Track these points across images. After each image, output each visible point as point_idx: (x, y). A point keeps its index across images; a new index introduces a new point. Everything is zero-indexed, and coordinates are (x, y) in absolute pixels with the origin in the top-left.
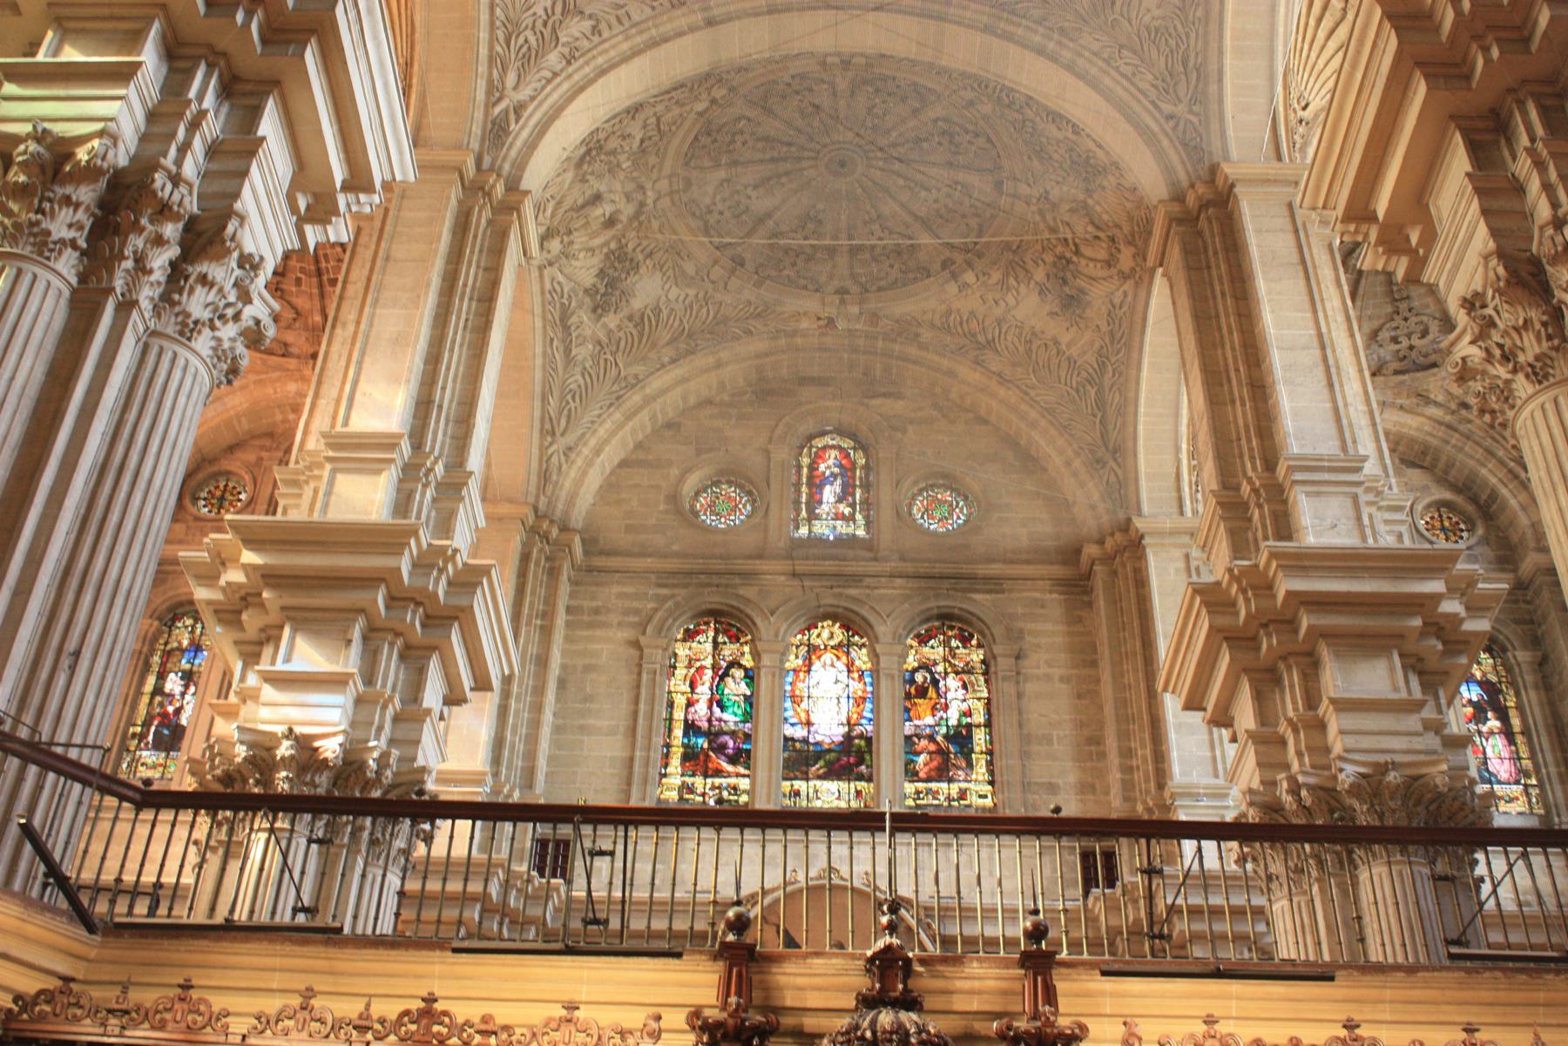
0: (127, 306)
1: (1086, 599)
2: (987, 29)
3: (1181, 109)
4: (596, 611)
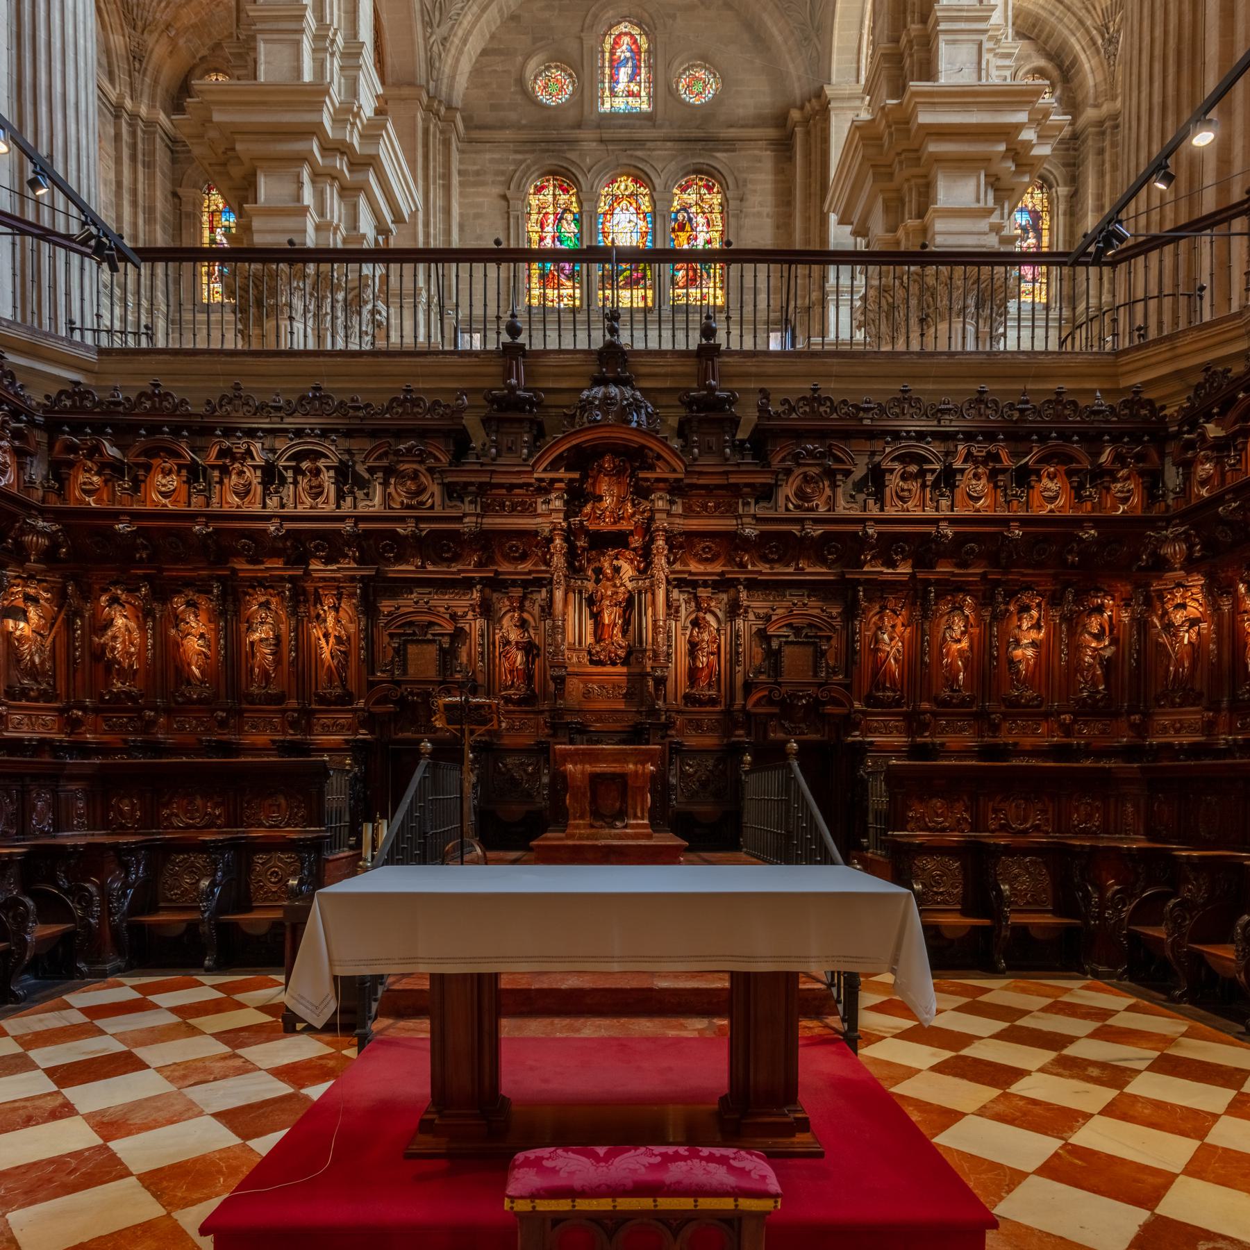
4: (477, 173)
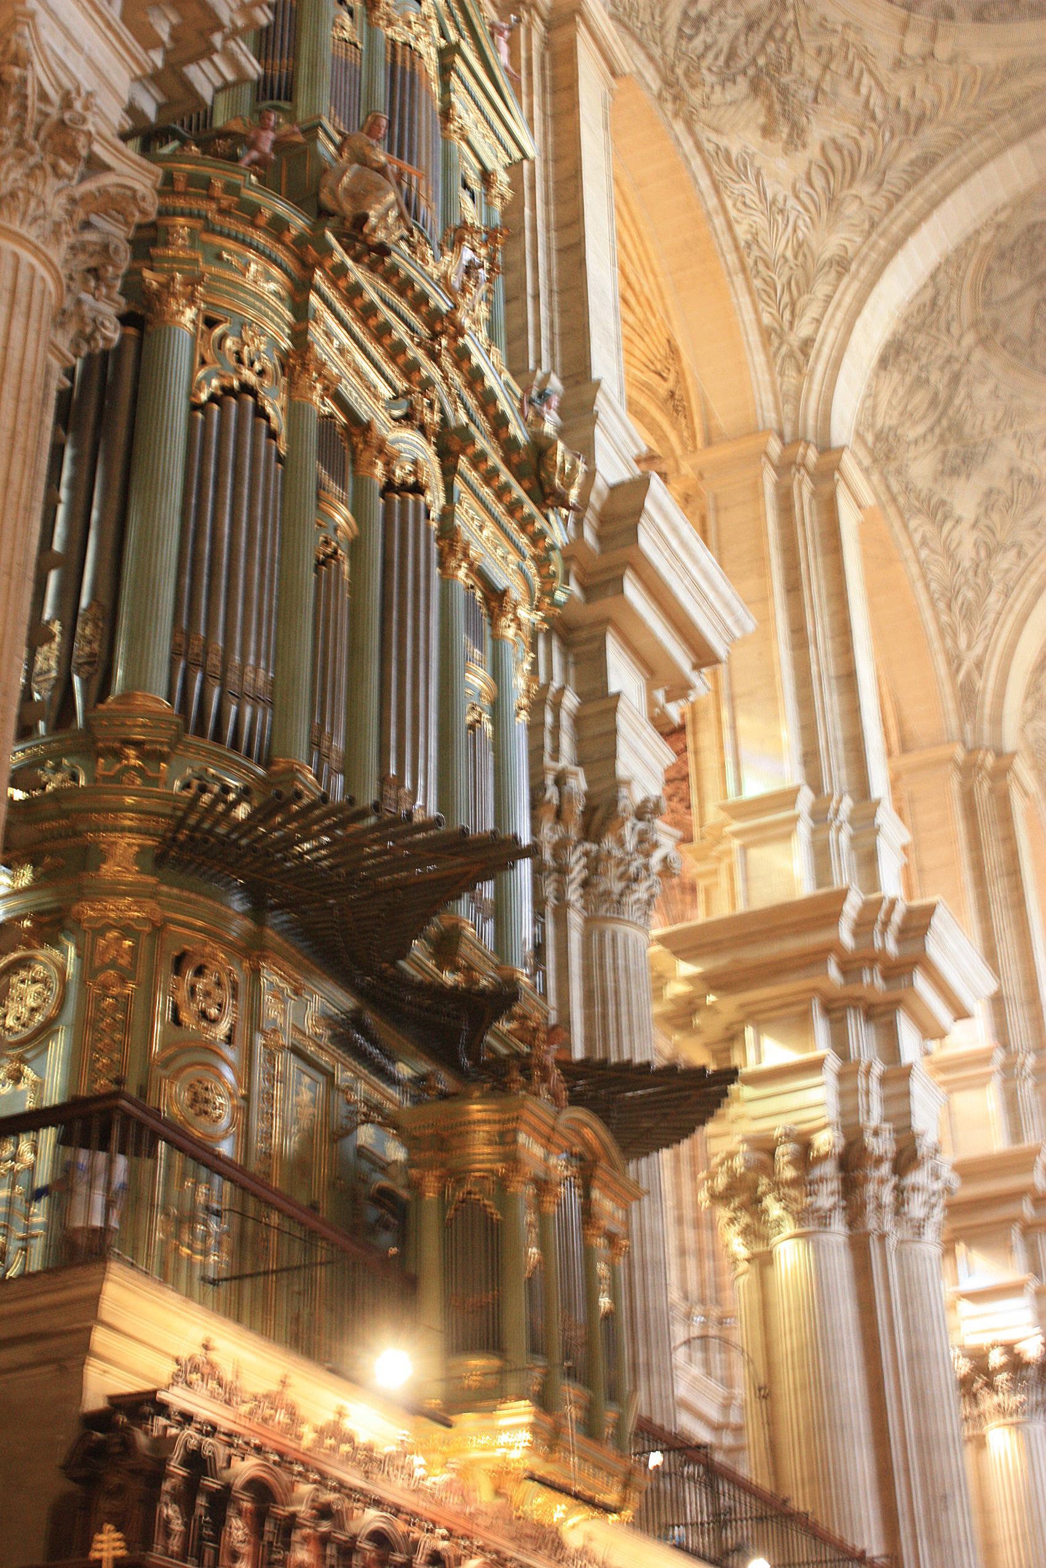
0: (882, 1237)
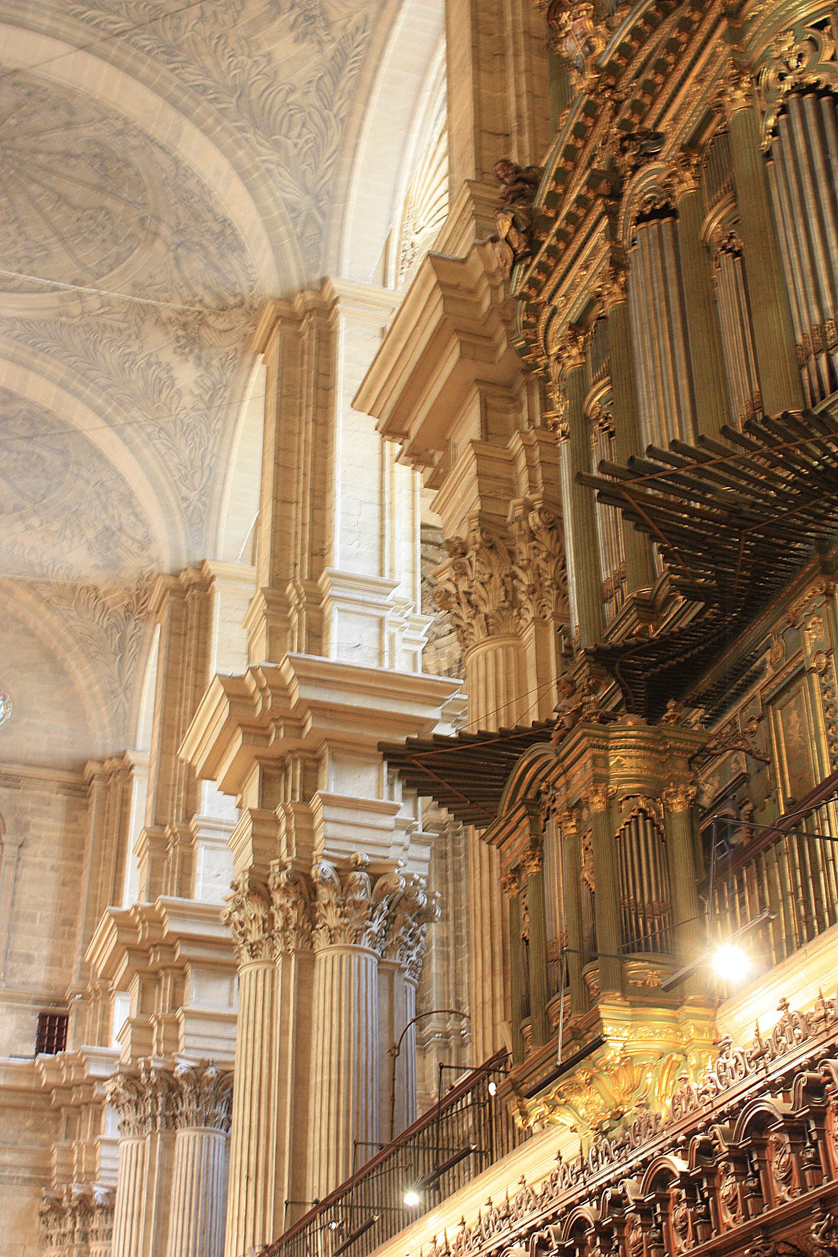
1: (84, 801)
2: (62, 385)
3: (193, 496)
